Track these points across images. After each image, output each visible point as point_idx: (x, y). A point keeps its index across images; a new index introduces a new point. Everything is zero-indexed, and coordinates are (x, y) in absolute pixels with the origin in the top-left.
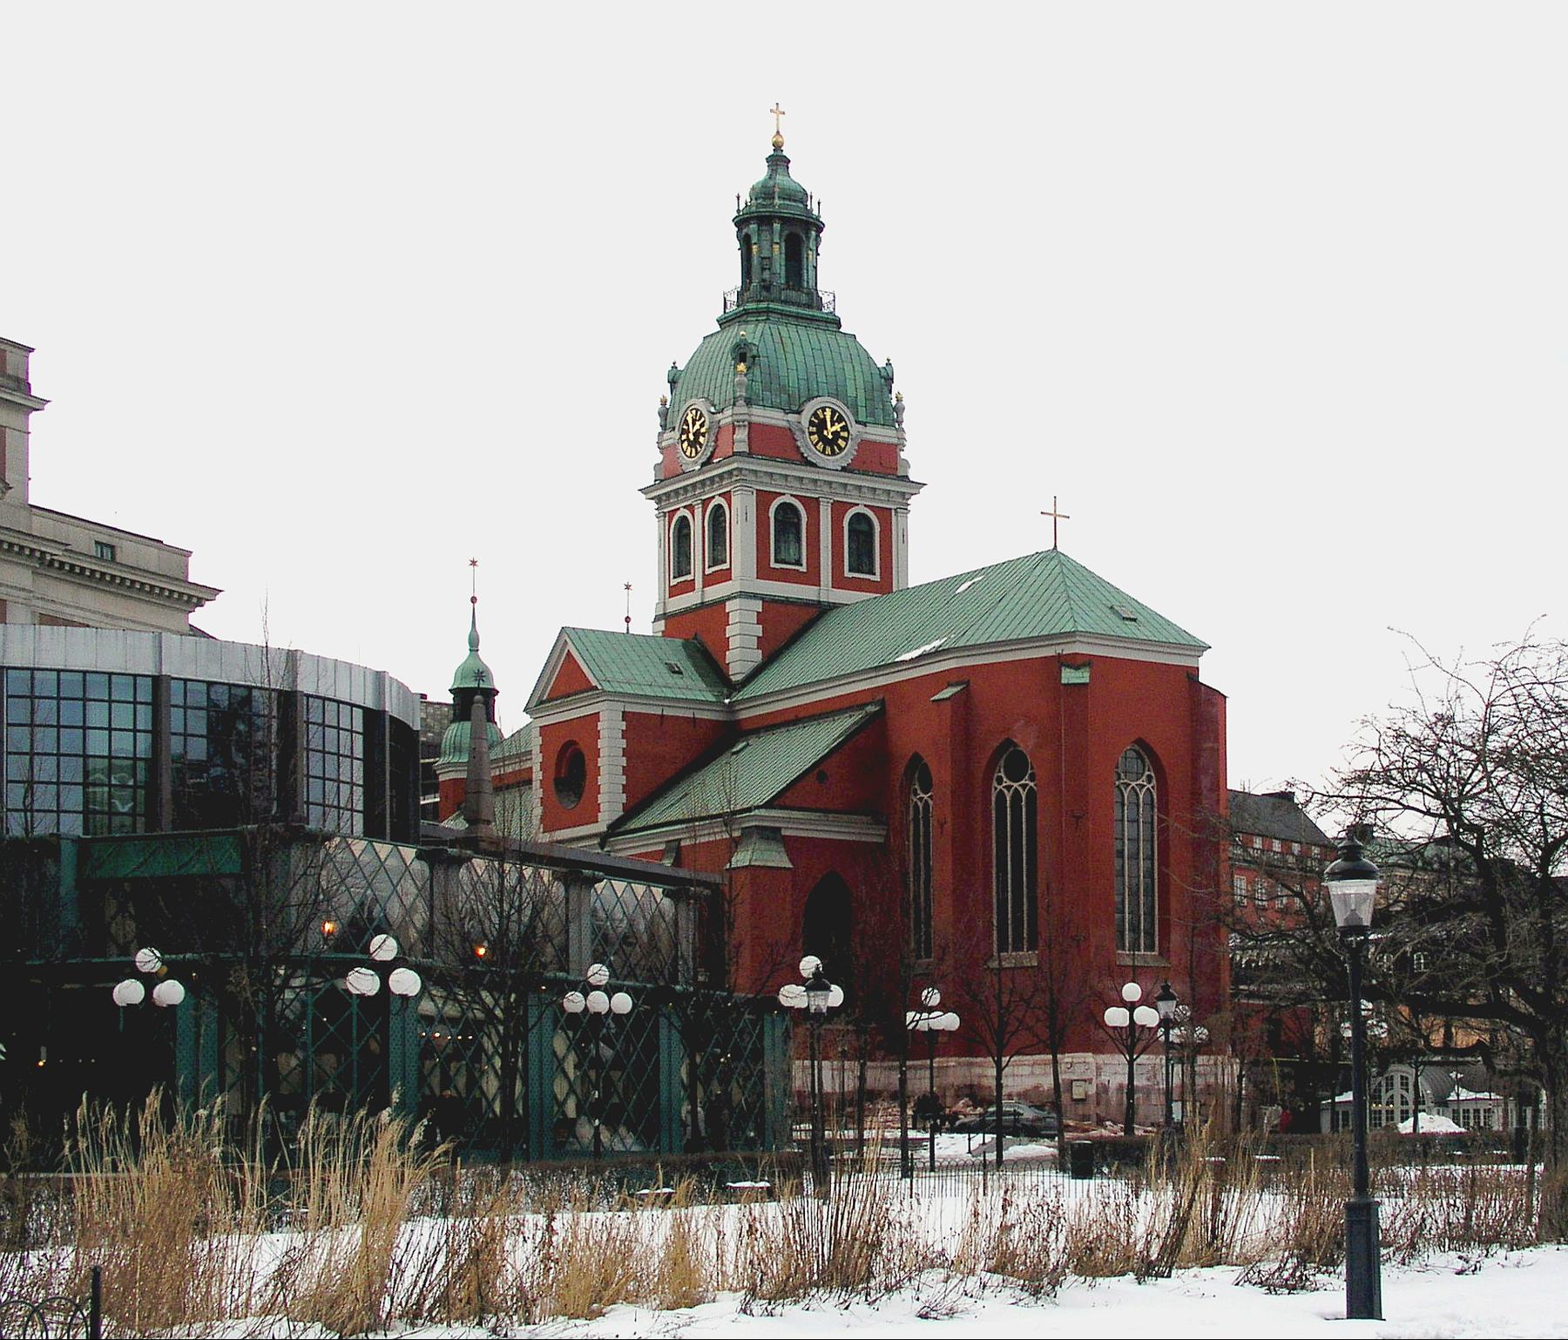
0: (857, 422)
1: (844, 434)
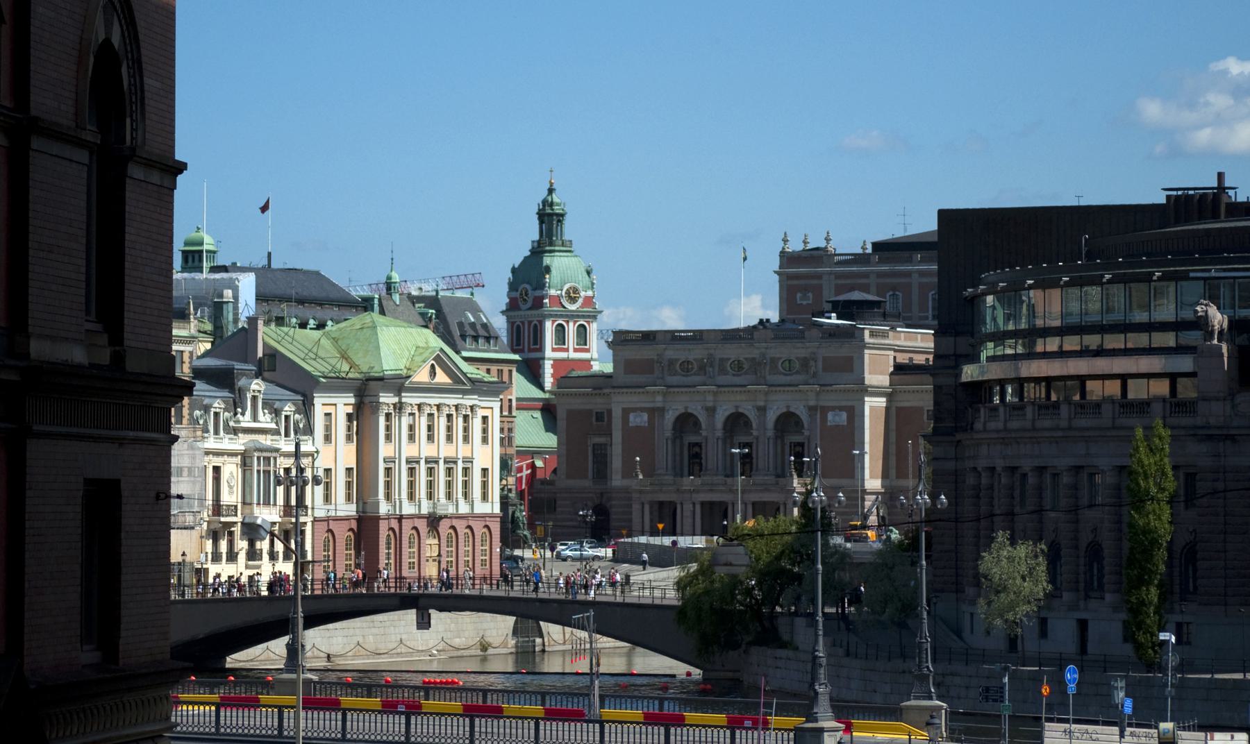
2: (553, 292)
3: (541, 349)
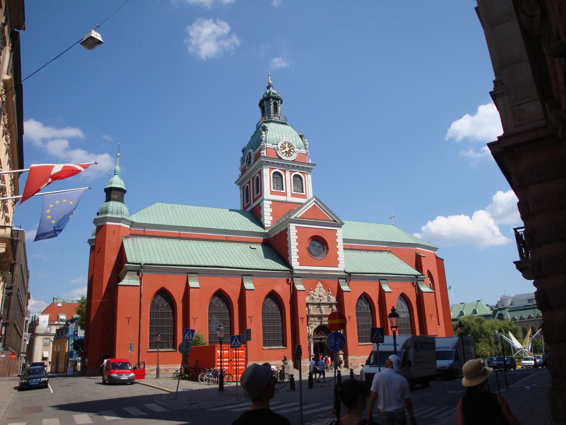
0: (297, 148)
1: (293, 151)
2: (269, 145)
3: (261, 195)
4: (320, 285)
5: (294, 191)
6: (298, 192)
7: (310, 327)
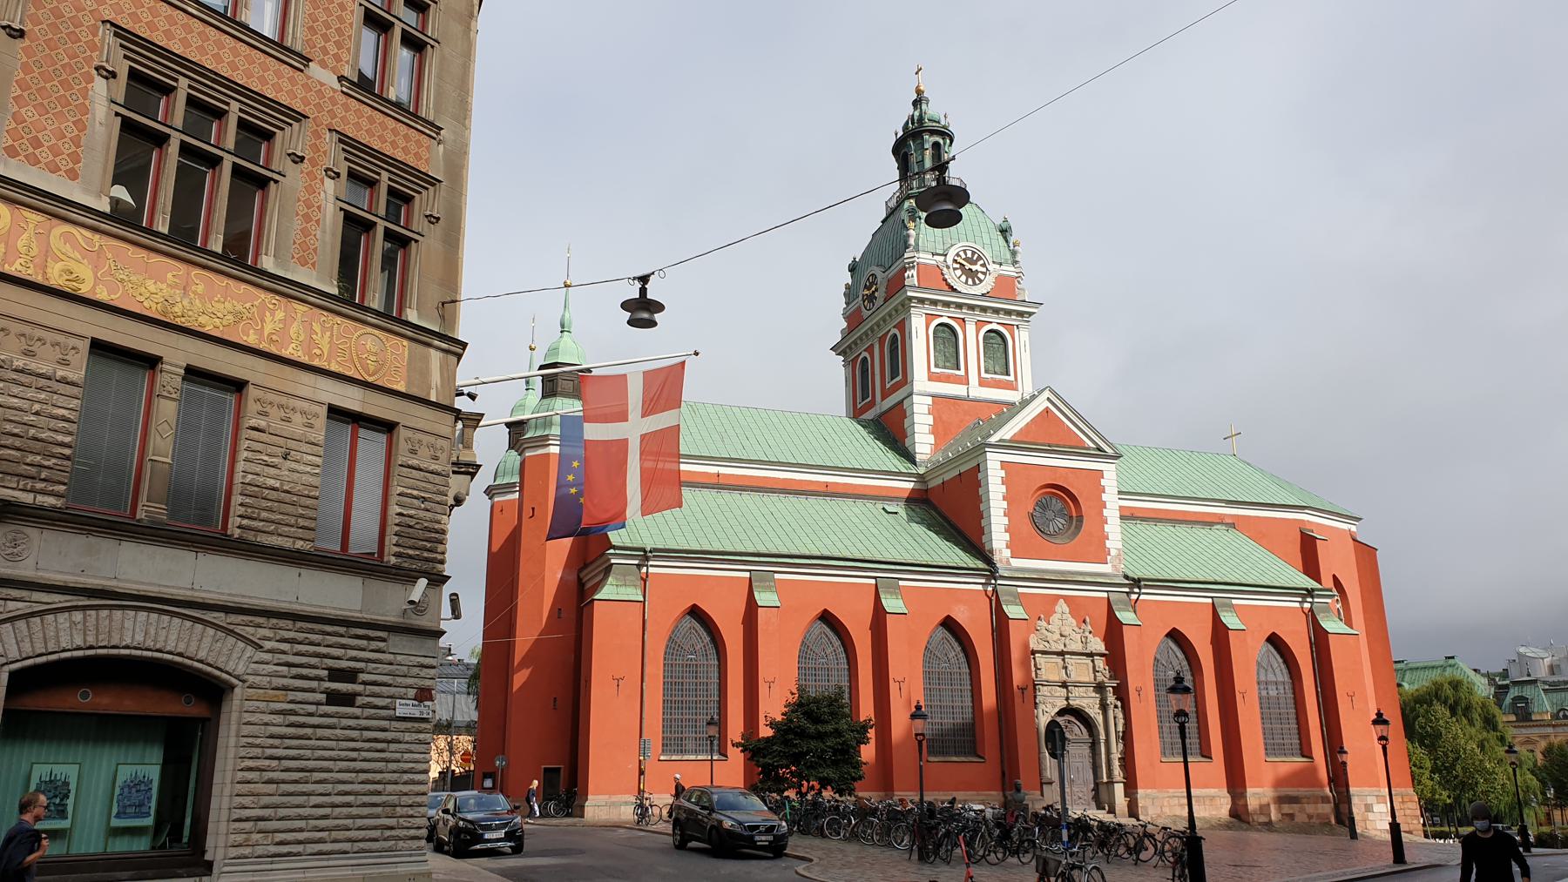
0: (994, 262)
2: (924, 258)
3: (906, 381)
4: (1062, 607)
5: (987, 371)
6: (995, 373)
7: (1040, 711)
